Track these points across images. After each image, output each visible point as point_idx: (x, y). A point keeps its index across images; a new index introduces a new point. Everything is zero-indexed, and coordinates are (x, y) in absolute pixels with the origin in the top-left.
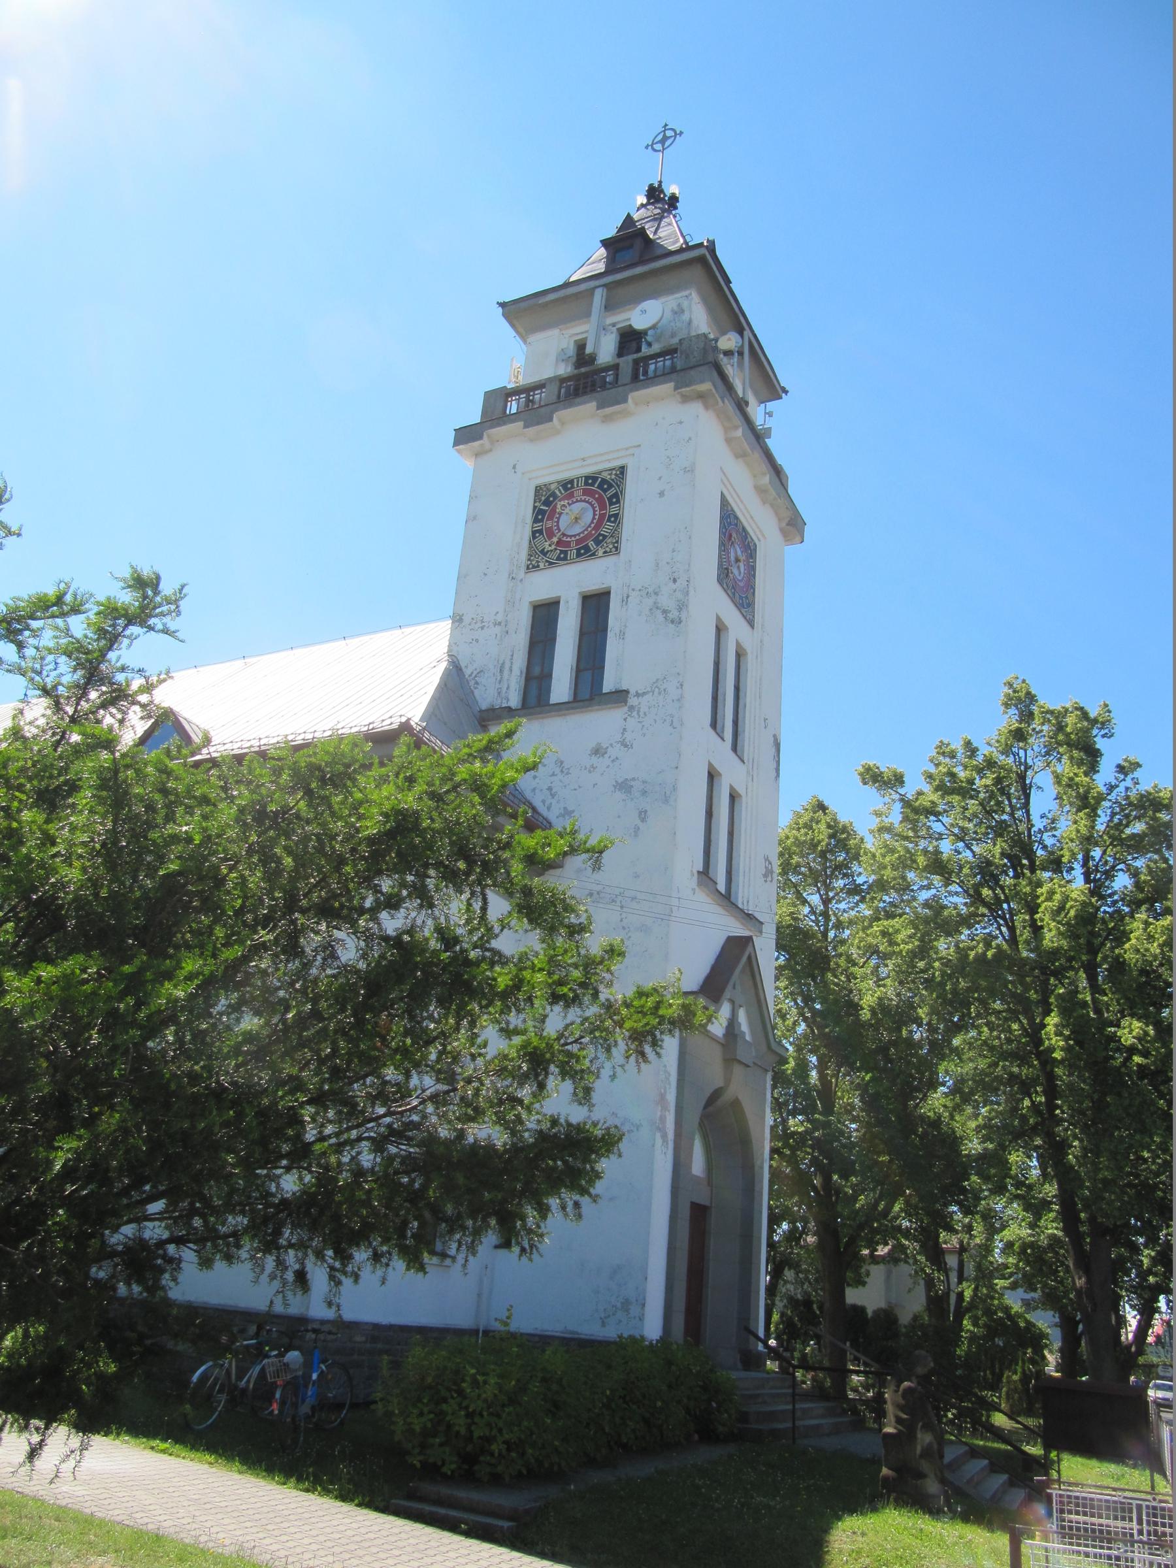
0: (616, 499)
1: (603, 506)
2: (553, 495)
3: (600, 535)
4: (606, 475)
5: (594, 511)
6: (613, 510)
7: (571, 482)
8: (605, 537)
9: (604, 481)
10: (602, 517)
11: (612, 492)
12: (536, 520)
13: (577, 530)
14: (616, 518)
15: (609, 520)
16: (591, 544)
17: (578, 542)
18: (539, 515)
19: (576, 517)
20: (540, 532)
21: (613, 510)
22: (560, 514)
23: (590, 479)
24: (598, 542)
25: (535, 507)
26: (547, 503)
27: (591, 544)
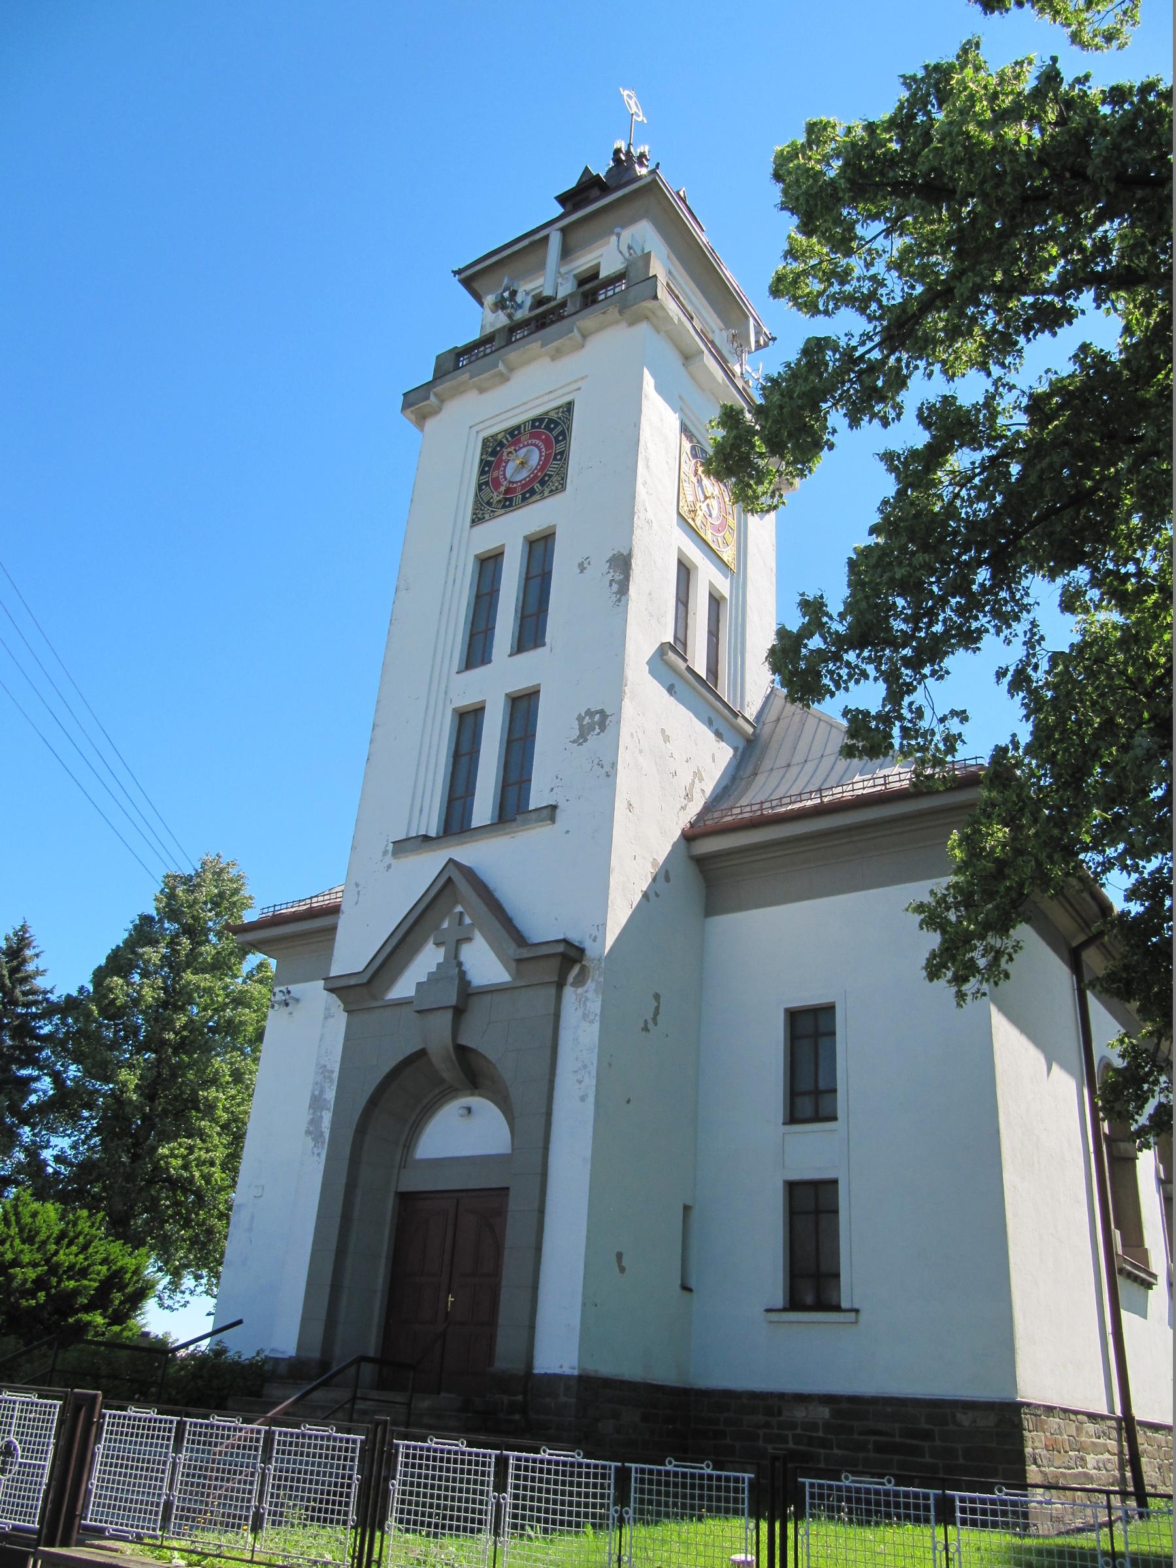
0: (564, 435)
1: (548, 445)
2: (501, 444)
3: (546, 475)
4: (553, 415)
5: (541, 452)
6: (559, 448)
7: (518, 427)
8: (550, 476)
9: (551, 421)
10: (547, 457)
11: (559, 429)
12: (482, 472)
13: (524, 474)
14: (563, 456)
15: (555, 459)
16: (537, 486)
17: (523, 486)
18: (486, 467)
19: (520, 465)
20: (487, 483)
21: (559, 448)
22: (507, 463)
23: (537, 421)
24: (543, 483)
25: (481, 460)
26: (494, 453)
27: (537, 486)
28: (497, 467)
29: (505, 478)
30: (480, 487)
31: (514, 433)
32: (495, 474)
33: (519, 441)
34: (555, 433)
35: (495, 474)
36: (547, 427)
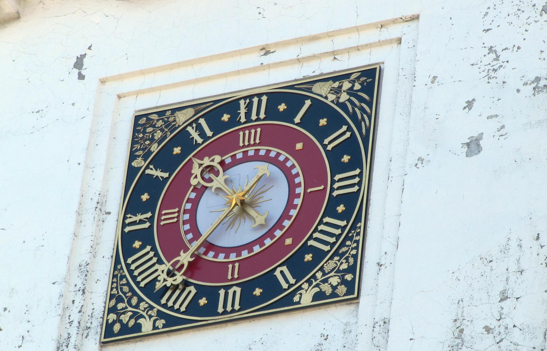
0: (355, 154)
1: (313, 175)
3: (306, 249)
4: (322, 90)
5: (292, 186)
6: (342, 184)
7: (231, 105)
8: (319, 255)
9: (319, 108)
10: (311, 202)
11: (341, 135)
12: (132, 205)
13: (243, 234)
14: (352, 209)
15: (331, 212)
16: (283, 275)
17: (246, 266)
18: (141, 193)
20: (146, 237)
21: (342, 184)
22: (200, 191)
23: (283, 101)
25: (131, 172)
26: (165, 160)
27: (283, 275)
28: (175, 200)
29: (197, 234)
30: (127, 242)
31: (221, 113)
32: (169, 216)
33: (230, 144)
34: (332, 141)
35: (169, 216)
36: (309, 122)
